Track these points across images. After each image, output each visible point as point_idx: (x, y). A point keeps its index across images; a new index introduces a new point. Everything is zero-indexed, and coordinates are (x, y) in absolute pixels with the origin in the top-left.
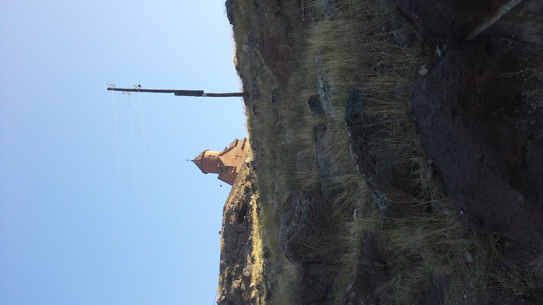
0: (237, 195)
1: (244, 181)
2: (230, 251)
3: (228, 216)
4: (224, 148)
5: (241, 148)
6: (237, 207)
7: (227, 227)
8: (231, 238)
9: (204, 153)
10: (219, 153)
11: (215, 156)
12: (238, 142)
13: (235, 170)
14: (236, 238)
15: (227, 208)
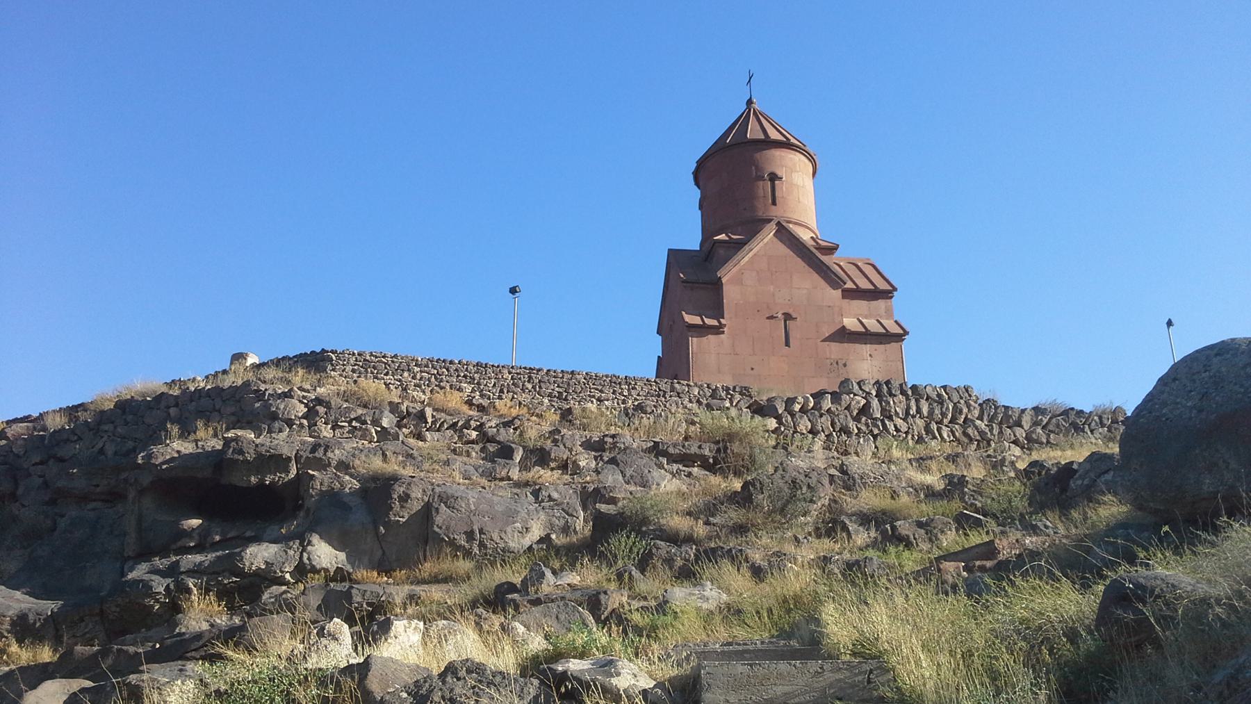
0: (376, 422)
1: (507, 435)
2: (62, 460)
3: (233, 396)
4: (827, 238)
5: (844, 326)
6: (241, 452)
7: (173, 411)
8: (110, 450)
9: (787, 145)
10: (795, 217)
11: (774, 203)
12: (881, 304)
13: (703, 330)
14: (98, 490)
15: (299, 377)
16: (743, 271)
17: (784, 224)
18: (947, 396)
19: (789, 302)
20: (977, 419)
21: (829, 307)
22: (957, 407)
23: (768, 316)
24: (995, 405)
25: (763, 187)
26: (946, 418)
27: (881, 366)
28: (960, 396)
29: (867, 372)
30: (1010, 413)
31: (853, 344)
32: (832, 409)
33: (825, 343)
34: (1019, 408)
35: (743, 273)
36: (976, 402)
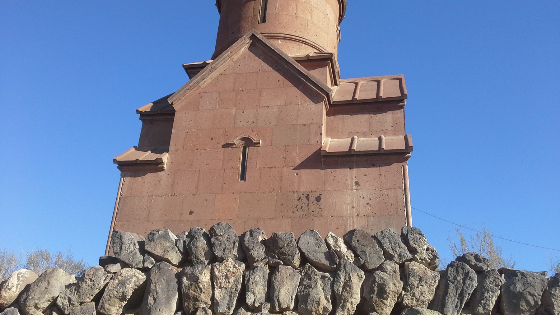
11: (264, 21)
16: (202, 94)
17: (258, 36)
18: (350, 256)
19: (253, 125)
20: (431, 306)
21: (305, 125)
22: (374, 281)
23: (223, 143)
24: (480, 272)
25: (254, 6)
26: (343, 307)
27: (371, 196)
28: (385, 253)
29: (349, 207)
30: (519, 287)
31: (334, 169)
32: (59, 299)
33: (294, 170)
34: (543, 274)
35: (201, 97)
36: (432, 265)
